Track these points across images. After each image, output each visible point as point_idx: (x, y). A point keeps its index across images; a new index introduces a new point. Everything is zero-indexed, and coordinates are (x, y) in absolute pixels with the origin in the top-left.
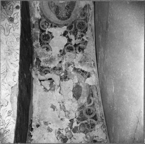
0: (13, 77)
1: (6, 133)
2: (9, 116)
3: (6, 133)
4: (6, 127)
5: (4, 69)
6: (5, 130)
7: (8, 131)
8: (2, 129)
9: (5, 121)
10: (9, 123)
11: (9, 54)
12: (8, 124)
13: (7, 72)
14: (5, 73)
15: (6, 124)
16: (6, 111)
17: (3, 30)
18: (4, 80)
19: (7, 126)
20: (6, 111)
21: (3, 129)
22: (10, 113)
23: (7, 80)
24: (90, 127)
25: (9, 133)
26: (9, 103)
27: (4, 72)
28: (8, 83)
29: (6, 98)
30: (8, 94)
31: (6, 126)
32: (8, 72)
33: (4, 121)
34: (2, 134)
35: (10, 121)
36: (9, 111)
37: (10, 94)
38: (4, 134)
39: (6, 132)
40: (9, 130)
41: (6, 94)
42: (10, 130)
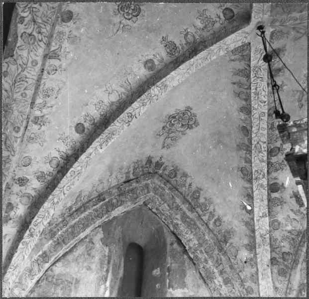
0: (8, 70)
5: (18, 86)
11: (7, 106)
13: (15, 81)
14: (19, 80)
15: (29, 8)
17: (7, 143)
18: (22, 71)
23: (18, 69)
26: (19, 35)
27: (19, 82)
28: (17, 64)
29: (23, 43)
30: (19, 48)
32: (14, 80)
33: (30, 13)
35: (22, 9)
37: (16, 48)
41: (22, 50)
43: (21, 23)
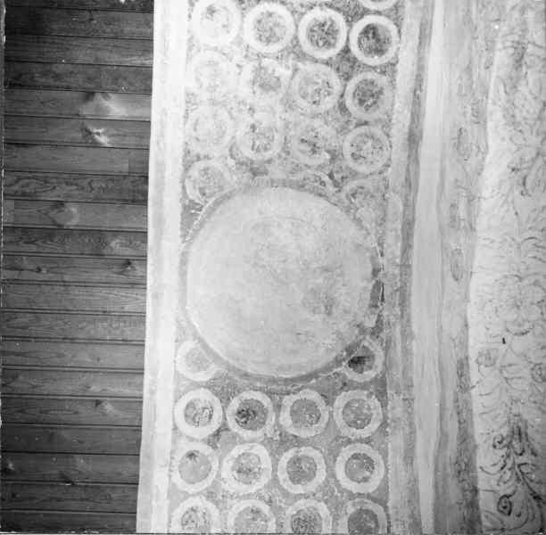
1: (503, 439)
2: (505, 496)
3: (503, 439)
4: (508, 456)
6: (508, 448)
7: (497, 444)
8: (519, 452)
9: (514, 477)
10: (499, 472)
12: (502, 468)
15: (510, 469)
16: (519, 516)
19: (505, 461)
20: (519, 516)
21: (516, 453)
22: (505, 507)
24: (200, 514)
25: (495, 439)
31: (507, 461)
33: (518, 479)
34: (517, 436)
36: (509, 514)
38: (507, 436)
39: (505, 442)
40: (495, 447)
42: (491, 448)
43: (506, 511)
